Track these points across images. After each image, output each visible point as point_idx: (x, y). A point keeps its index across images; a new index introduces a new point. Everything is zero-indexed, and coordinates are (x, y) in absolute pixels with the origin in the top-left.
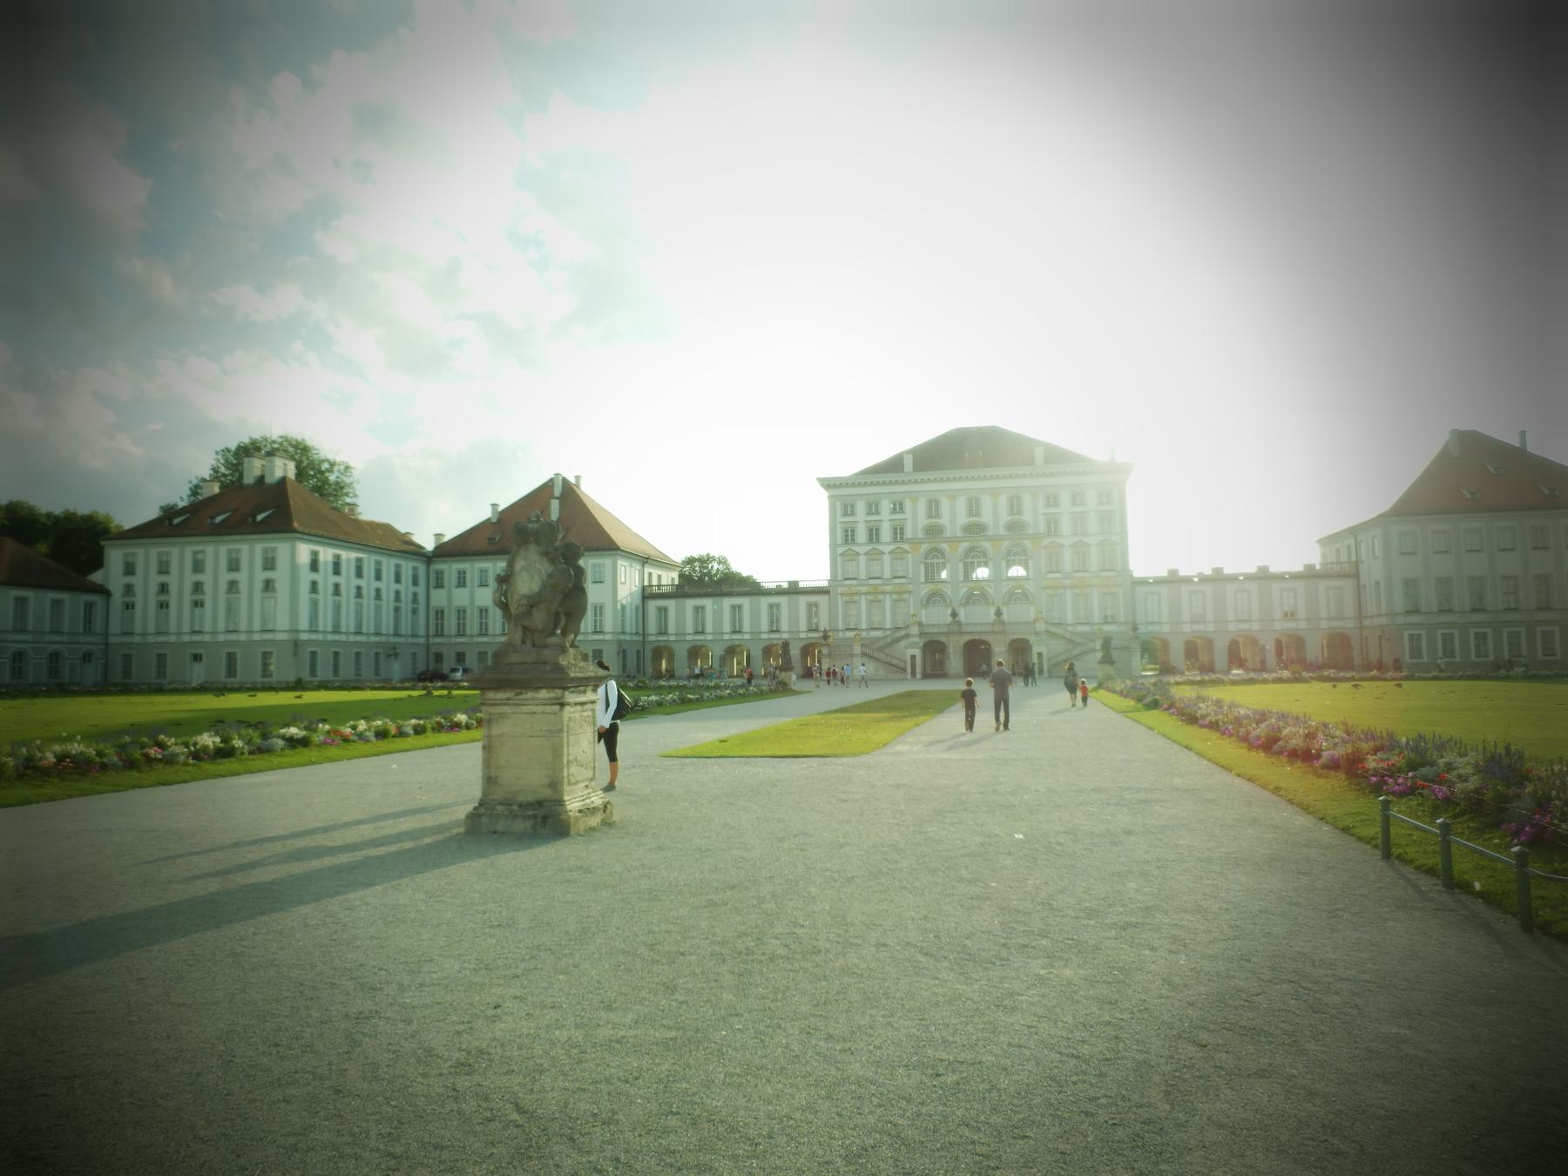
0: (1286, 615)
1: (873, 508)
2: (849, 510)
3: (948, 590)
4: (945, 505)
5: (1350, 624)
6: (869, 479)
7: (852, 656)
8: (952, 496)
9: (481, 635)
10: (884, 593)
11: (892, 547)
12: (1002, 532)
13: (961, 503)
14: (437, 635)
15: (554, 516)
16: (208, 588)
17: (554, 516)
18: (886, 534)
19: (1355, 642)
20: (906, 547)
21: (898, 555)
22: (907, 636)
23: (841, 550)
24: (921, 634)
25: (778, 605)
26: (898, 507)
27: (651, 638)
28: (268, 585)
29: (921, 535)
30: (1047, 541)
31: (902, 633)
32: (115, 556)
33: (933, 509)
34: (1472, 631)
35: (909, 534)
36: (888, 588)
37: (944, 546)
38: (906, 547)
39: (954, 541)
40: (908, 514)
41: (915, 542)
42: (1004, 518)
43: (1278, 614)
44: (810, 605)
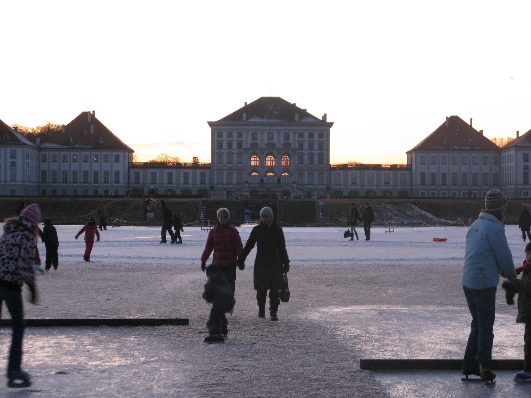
0: (386, 183)
2: (220, 135)
4: (259, 134)
5: (408, 187)
11: (236, 151)
12: (281, 147)
13: (266, 135)
14: (43, 182)
17: (92, 132)
18: (235, 146)
20: (243, 151)
21: (240, 155)
23: (216, 151)
24: (249, 187)
26: (240, 135)
27: (132, 185)
28: (13, 164)
29: (249, 147)
30: (298, 152)
34: (441, 192)
35: (244, 146)
40: (244, 138)
41: (246, 150)
42: (282, 141)
44: (201, 173)
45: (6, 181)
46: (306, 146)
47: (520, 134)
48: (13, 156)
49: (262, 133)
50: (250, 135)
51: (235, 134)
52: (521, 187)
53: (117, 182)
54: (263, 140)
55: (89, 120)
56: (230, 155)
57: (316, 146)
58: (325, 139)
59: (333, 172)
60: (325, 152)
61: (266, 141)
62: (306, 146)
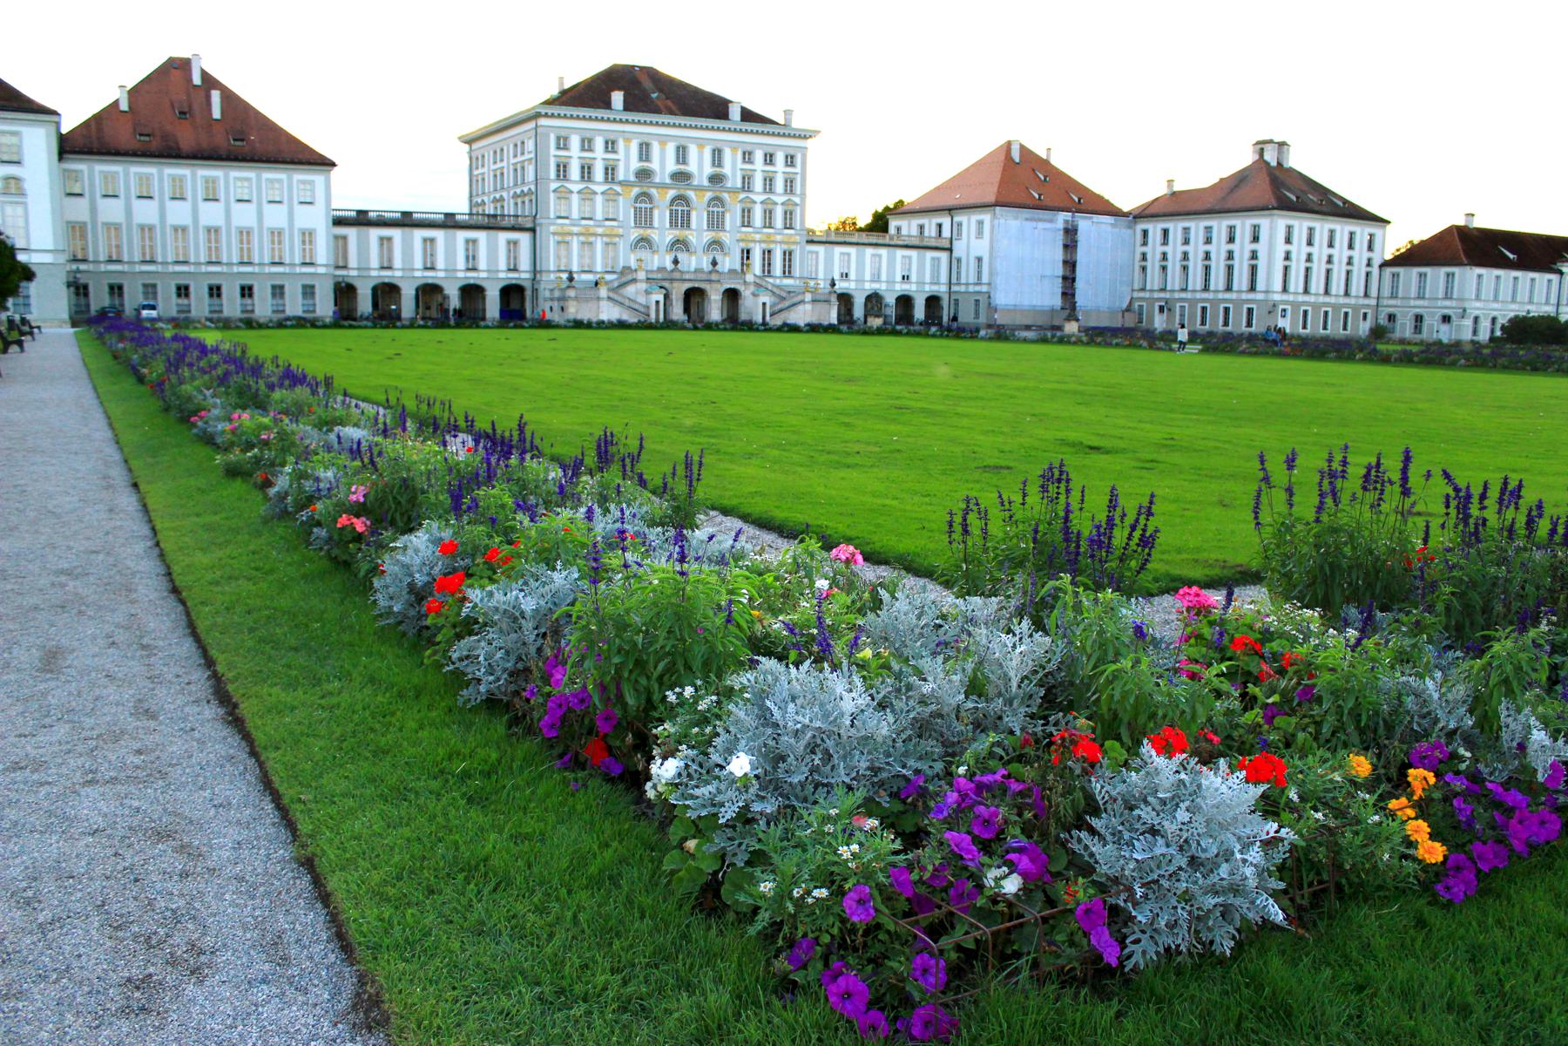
1: (587, 144)
3: (654, 235)
5: (944, 288)
6: (556, 110)
7: (599, 299)
8: (664, 141)
9: (110, 261)
10: (595, 235)
12: (706, 183)
15: (217, 114)
17: (217, 114)
18: (599, 174)
19: (945, 304)
21: (610, 197)
22: (634, 281)
23: (554, 186)
25: (475, 241)
26: (610, 146)
29: (632, 178)
30: (742, 196)
31: (630, 277)
33: (645, 151)
35: (621, 176)
36: (600, 230)
37: (654, 191)
38: (618, 188)
39: (663, 187)
40: (621, 155)
42: (708, 170)
43: (899, 278)
46: (758, 184)
47: (1176, 188)
49: (663, 144)
51: (599, 143)
54: (664, 163)
55: (197, 80)
56: (587, 195)
57: (779, 185)
58: (798, 169)
60: (797, 200)
61: (672, 166)
62: (758, 184)
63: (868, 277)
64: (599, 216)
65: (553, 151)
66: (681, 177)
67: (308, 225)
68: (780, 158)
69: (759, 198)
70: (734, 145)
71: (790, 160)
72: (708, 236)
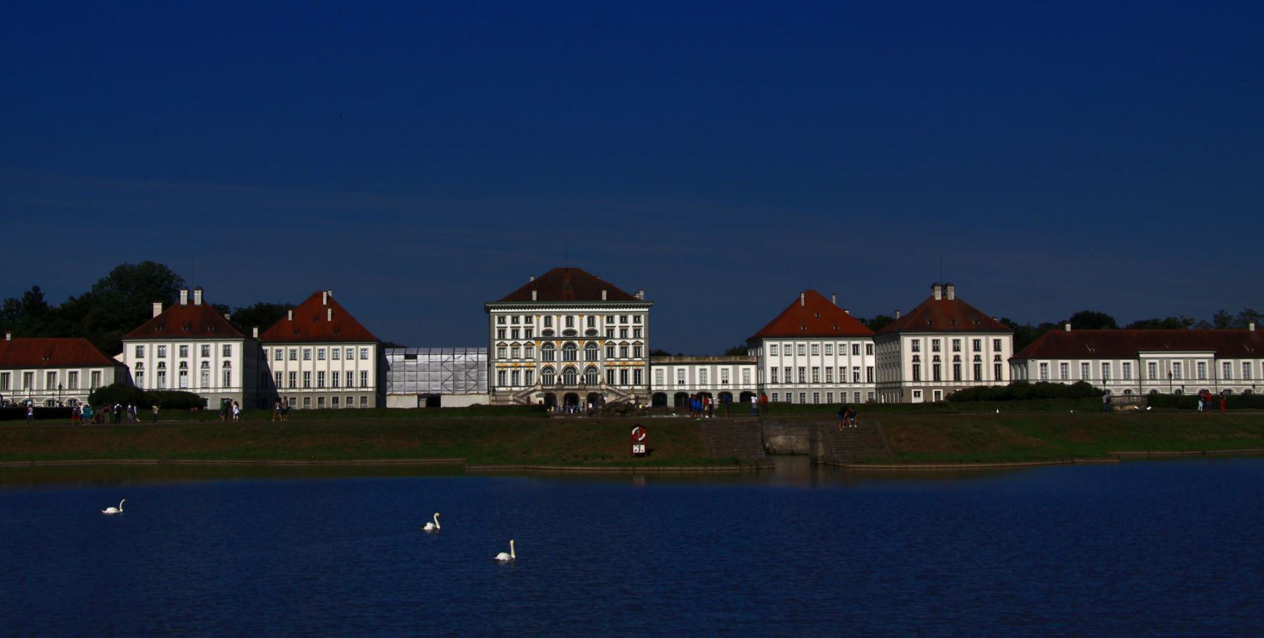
3: (555, 365)
4: (554, 318)
5: (753, 387)
8: (559, 314)
15: (329, 319)
16: (190, 365)
17: (329, 319)
18: (522, 334)
26: (528, 319)
28: (227, 364)
32: (130, 348)
33: (548, 321)
35: (535, 335)
39: (558, 339)
40: (535, 324)
41: (537, 339)
42: (586, 328)
45: (216, 388)
46: (617, 333)
48: (227, 352)
50: (542, 318)
52: (910, 385)
53: (364, 385)
54: (559, 325)
55: (325, 302)
56: (515, 347)
57: (630, 333)
59: (654, 368)
61: (563, 327)
62: (617, 333)
63: (698, 382)
64: (522, 356)
65: (496, 324)
66: (570, 333)
67: (364, 369)
68: (630, 318)
69: (617, 342)
70: (601, 314)
71: (637, 319)
72: (586, 364)
